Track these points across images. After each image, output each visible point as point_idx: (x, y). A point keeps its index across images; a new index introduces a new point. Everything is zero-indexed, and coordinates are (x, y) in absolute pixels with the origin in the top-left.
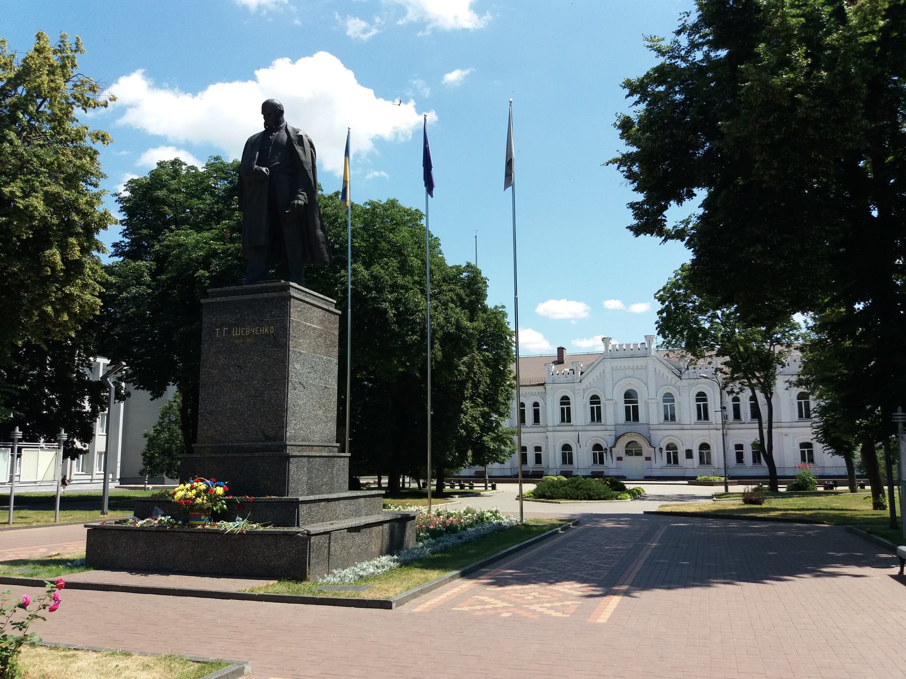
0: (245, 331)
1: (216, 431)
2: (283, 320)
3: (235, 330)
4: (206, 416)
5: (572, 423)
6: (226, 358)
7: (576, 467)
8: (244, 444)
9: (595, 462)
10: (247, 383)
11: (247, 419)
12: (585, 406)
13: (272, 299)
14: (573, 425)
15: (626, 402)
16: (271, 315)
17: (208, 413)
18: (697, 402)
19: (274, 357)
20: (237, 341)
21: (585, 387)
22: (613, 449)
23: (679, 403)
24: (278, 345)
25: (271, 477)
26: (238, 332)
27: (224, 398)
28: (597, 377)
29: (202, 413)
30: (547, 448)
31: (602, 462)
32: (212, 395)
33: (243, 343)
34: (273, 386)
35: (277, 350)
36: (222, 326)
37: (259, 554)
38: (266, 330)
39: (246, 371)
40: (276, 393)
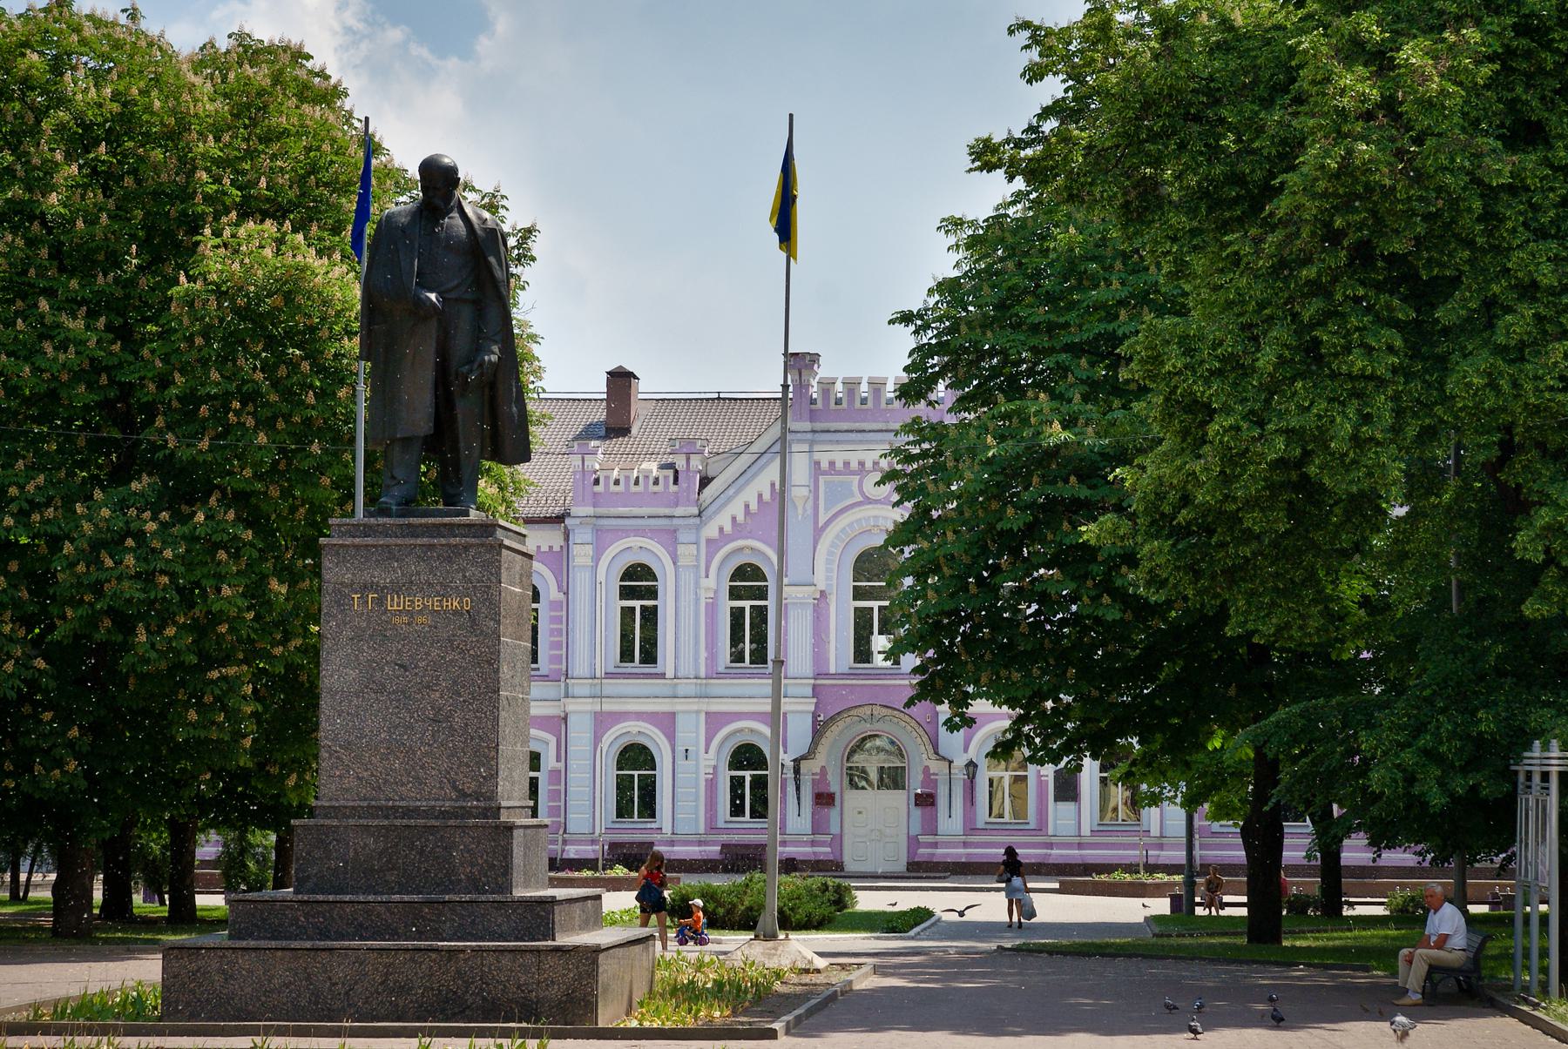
2: (489, 587)
3: (392, 600)
5: (659, 669)
6: (375, 649)
8: (418, 803)
9: (737, 810)
10: (419, 696)
13: (466, 548)
14: (662, 676)
15: (858, 594)
16: (464, 576)
20: (396, 620)
21: (714, 534)
22: (804, 765)
26: (399, 605)
27: (373, 722)
28: (760, 496)
30: (562, 753)
31: (760, 810)
36: (365, 588)
37: (508, 981)
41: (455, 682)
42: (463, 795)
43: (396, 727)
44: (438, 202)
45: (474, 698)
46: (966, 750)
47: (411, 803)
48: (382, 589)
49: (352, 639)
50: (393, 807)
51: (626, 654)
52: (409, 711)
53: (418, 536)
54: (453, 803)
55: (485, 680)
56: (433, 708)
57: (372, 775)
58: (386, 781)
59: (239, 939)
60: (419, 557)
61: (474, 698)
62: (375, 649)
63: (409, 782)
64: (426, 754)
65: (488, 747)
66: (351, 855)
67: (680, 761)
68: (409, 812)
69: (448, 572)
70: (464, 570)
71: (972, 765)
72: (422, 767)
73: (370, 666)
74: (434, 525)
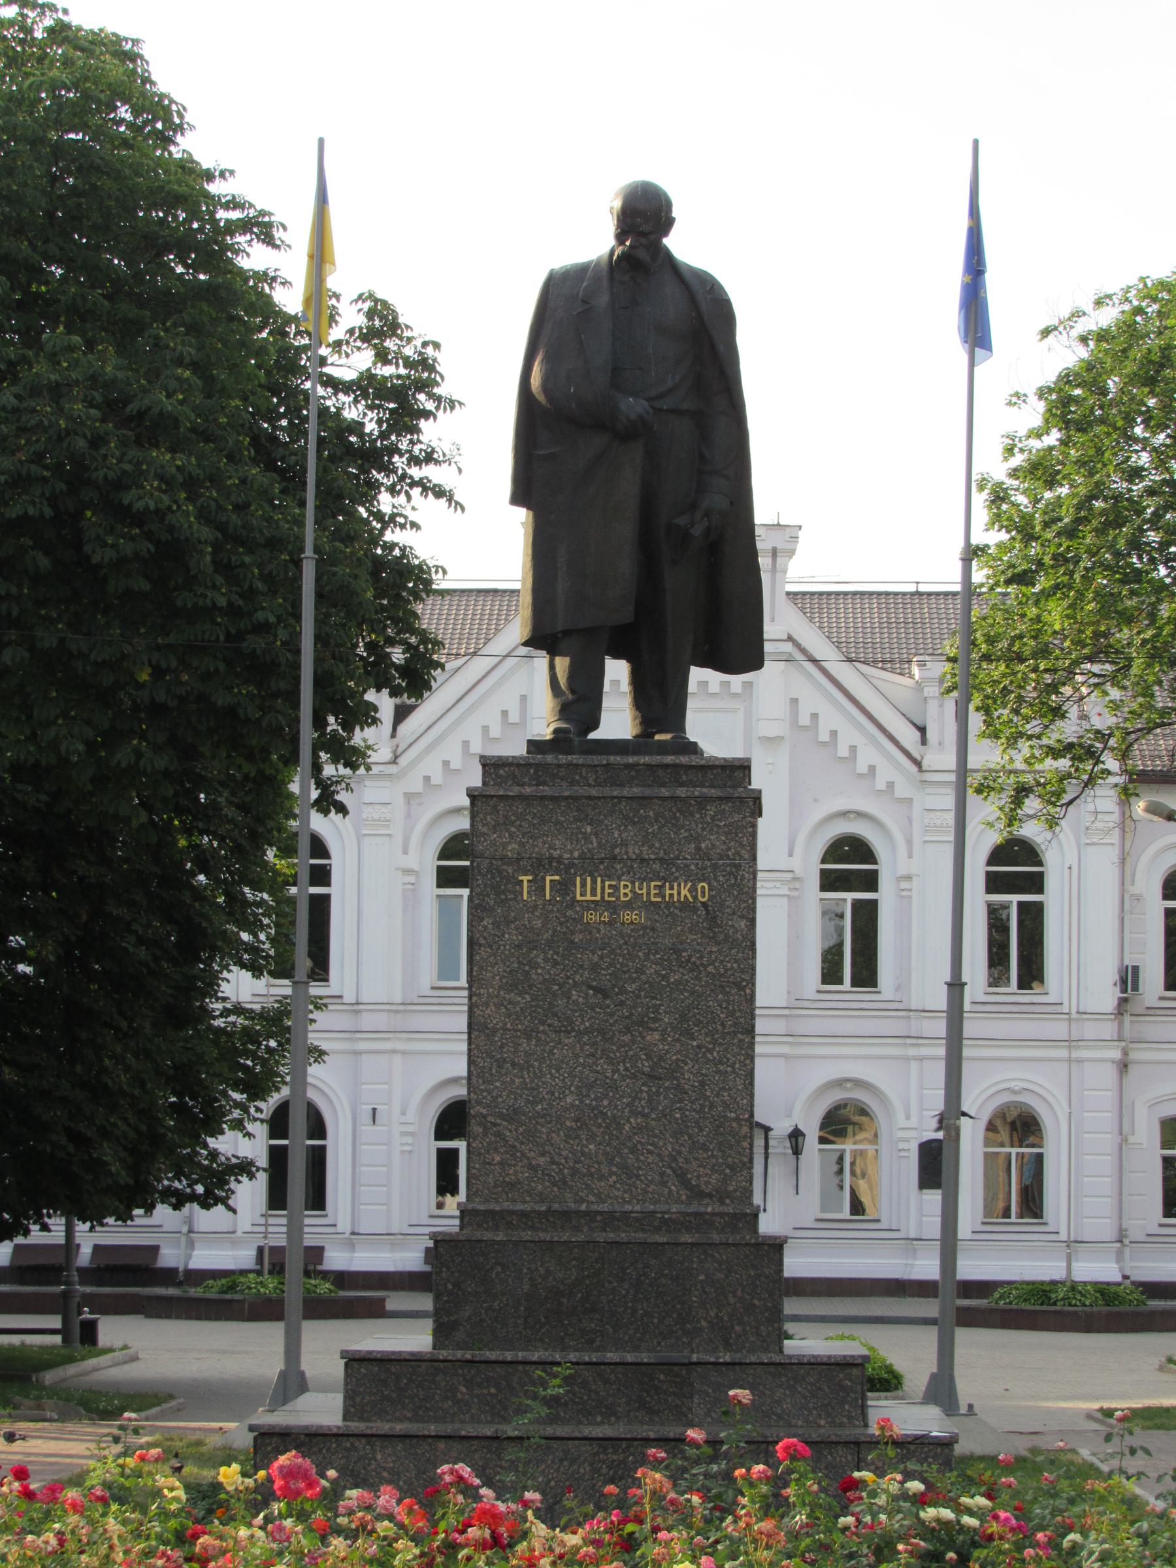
0: (615, 888)
1: (531, 1167)
2: (738, 867)
3: (583, 885)
4: (495, 1124)
6: (556, 963)
7: (344, 1225)
8: (628, 1208)
10: (627, 1038)
12: (411, 895)
13: (702, 802)
16: (698, 849)
17: (502, 1116)
18: (990, 890)
19: (711, 969)
20: (590, 917)
21: (417, 786)
23: (904, 898)
24: (722, 937)
25: (732, 1300)
26: (594, 893)
27: (553, 1078)
29: (484, 1117)
32: (514, 1065)
33: (611, 923)
34: (710, 1051)
35: (720, 952)
36: (539, 866)
38: (684, 892)
39: (622, 1003)
40: (718, 1072)
41: (683, 1017)
42: (698, 1194)
43: (591, 1086)
44: (642, 254)
46: (789, 1116)
47: (617, 1208)
49: (519, 947)
50: (587, 1213)
51: (831, 974)
52: (610, 1061)
53: (622, 785)
54: (683, 1208)
57: (553, 1162)
58: (574, 1172)
59: (362, 1419)
60: (626, 817)
62: (556, 963)
63: (611, 1173)
64: (639, 1129)
65: (738, 1119)
66: (526, 1287)
67: (367, 1129)
68: (611, 1219)
70: (698, 839)
71: (796, 1135)
72: (633, 1150)
74: (649, 766)
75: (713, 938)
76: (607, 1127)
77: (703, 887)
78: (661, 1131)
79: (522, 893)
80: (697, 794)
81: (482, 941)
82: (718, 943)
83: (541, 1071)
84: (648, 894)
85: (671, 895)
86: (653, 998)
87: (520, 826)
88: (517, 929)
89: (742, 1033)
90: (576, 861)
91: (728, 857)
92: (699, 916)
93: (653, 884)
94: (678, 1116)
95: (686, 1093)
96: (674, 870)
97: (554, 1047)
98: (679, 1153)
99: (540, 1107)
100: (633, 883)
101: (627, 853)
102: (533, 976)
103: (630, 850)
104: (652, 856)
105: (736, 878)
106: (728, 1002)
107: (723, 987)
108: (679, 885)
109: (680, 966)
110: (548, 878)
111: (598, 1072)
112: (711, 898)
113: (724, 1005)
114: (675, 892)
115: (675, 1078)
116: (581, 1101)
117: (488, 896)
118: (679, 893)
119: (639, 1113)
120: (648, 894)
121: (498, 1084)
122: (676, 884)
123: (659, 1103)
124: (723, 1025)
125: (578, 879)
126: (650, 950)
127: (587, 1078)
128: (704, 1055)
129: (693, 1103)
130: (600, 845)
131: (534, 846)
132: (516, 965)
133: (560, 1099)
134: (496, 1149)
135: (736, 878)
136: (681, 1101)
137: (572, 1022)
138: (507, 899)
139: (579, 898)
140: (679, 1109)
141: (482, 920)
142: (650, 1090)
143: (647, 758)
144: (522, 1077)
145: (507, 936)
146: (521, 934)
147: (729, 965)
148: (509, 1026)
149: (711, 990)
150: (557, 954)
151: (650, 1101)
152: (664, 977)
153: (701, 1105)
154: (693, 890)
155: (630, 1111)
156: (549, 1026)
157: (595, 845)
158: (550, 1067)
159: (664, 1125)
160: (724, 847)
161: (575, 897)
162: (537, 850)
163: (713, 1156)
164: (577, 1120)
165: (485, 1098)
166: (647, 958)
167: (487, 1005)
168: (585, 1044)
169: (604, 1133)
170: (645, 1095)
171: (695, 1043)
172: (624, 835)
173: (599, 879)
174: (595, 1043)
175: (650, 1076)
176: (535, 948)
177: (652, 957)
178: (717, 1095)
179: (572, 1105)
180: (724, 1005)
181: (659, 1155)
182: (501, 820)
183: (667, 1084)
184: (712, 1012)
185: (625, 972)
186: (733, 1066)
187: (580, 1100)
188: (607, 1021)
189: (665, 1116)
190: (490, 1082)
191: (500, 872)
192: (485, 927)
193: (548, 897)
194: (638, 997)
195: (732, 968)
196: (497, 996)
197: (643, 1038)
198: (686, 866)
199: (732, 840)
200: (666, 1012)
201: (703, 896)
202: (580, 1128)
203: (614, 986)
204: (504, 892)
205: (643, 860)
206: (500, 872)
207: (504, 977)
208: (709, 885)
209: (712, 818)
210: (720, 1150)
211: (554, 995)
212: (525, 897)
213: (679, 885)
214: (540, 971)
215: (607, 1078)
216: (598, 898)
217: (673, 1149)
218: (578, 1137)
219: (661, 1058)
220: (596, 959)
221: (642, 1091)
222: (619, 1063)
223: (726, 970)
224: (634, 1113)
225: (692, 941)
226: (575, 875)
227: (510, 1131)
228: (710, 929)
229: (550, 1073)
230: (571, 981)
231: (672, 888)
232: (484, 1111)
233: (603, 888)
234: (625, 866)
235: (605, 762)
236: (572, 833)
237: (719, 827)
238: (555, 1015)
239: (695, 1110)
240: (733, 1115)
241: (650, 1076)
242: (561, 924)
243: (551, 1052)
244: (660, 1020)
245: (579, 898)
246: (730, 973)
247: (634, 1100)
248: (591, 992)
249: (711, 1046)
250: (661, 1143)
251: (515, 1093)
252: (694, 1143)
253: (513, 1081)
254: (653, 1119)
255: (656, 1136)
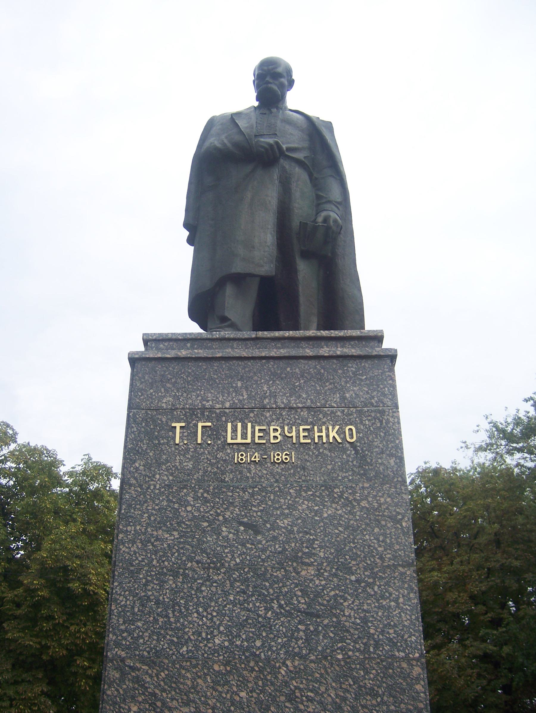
2: (382, 412)
3: (234, 430)
4: (133, 668)
6: (206, 501)
10: (280, 574)
11: (286, 684)
16: (343, 398)
17: (143, 660)
24: (373, 474)
26: (244, 436)
29: (123, 660)
32: (158, 603)
35: (372, 488)
38: (333, 434)
41: (339, 552)
43: (242, 625)
45: (374, 576)
48: (219, 417)
49: (169, 486)
52: (263, 598)
55: (391, 545)
56: (305, 593)
61: (374, 576)
64: (297, 673)
65: (407, 659)
69: (319, 393)
73: (198, 526)
75: (365, 474)
76: (261, 671)
77: (350, 430)
78: (321, 674)
79: (174, 438)
80: (339, 353)
81: (133, 481)
82: (369, 480)
83: (187, 610)
84: (298, 437)
85: (320, 437)
86: (306, 533)
87: (176, 382)
88: (167, 470)
89: (403, 566)
90: (227, 411)
91: (372, 404)
92: (349, 456)
93: (301, 428)
94: (340, 657)
95: (348, 631)
96: (321, 416)
97: (202, 584)
98: (344, 699)
99: (185, 649)
100: (283, 428)
101: (276, 402)
102: (182, 514)
103: (279, 401)
104: (300, 405)
105: (381, 422)
106: (385, 535)
107: (378, 520)
108: (327, 429)
109: (332, 502)
110: (200, 425)
111: (249, 610)
112: (359, 439)
113: (381, 538)
114: (324, 434)
115: (335, 615)
116: (231, 642)
117: (142, 441)
118: (328, 436)
119: (296, 654)
120: (298, 437)
121: (139, 624)
122: (324, 428)
123: (317, 642)
124: (381, 558)
125: (229, 425)
126: (301, 486)
127: (238, 617)
128: (364, 590)
129: (355, 642)
130: (250, 397)
131: (187, 399)
132: (165, 503)
133: (208, 640)
134: (133, 697)
135: (381, 422)
136: (342, 640)
137: (222, 558)
138: (159, 444)
139: (229, 441)
140: (341, 649)
141: (135, 462)
142: (307, 629)
143: (291, 332)
144: (167, 616)
145: (158, 476)
146: (172, 474)
147: (382, 500)
148: (155, 562)
149: (367, 524)
150: (208, 492)
151: (307, 640)
152: (316, 513)
153: (365, 644)
154: (341, 432)
155: (286, 653)
156: (198, 562)
157: (246, 397)
158: (197, 605)
159: (325, 668)
160: (368, 396)
161: (226, 441)
162: (190, 401)
163: (383, 702)
164: (227, 663)
165: (125, 639)
166: (299, 495)
167: (133, 542)
168: (235, 580)
169: (257, 678)
170: (301, 633)
171: (353, 578)
172: (273, 389)
173: (249, 425)
174: (247, 580)
175: (307, 614)
176: (185, 487)
177: (304, 494)
178: (382, 632)
179: (221, 647)
180: (381, 538)
181: (321, 703)
182: (158, 378)
183: (326, 622)
184: (369, 546)
185: (277, 509)
186: (396, 600)
187: (229, 641)
188: (259, 557)
189: (325, 658)
190: (132, 622)
191: (154, 421)
192: (137, 469)
193: (199, 441)
194: (291, 532)
195: (386, 502)
196: (144, 534)
197: (298, 573)
198: (332, 412)
199: (374, 390)
200: (321, 547)
201: (352, 438)
202: (229, 672)
203: (266, 522)
204: (157, 438)
205: (291, 408)
206: (154, 421)
207: (152, 514)
208: (356, 429)
209: (354, 373)
210: (390, 695)
211: (204, 531)
212: (177, 441)
213: (327, 429)
214: (189, 508)
215: (259, 616)
216: (249, 441)
217: (337, 695)
218: (227, 683)
219: (318, 595)
220: (246, 497)
221: (298, 630)
222: (272, 600)
223: (380, 505)
224: (293, 656)
225: (343, 478)
226: (226, 422)
227: (151, 676)
228: (360, 467)
229: (197, 612)
230: (221, 518)
231: (320, 431)
232: (123, 654)
233: (253, 433)
234: (274, 413)
235: (254, 336)
236: (224, 388)
237: (361, 380)
238: (203, 551)
239: (359, 650)
240: (402, 654)
241: (307, 614)
242: (212, 465)
243: (199, 590)
244: (315, 554)
245: (229, 441)
246: (384, 507)
247: (290, 641)
248: (242, 528)
249: (371, 580)
250: (323, 689)
251: (159, 634)
252: (360, 687)
253: (156, 621)
254: (312, 661)
255: (316, 681)
